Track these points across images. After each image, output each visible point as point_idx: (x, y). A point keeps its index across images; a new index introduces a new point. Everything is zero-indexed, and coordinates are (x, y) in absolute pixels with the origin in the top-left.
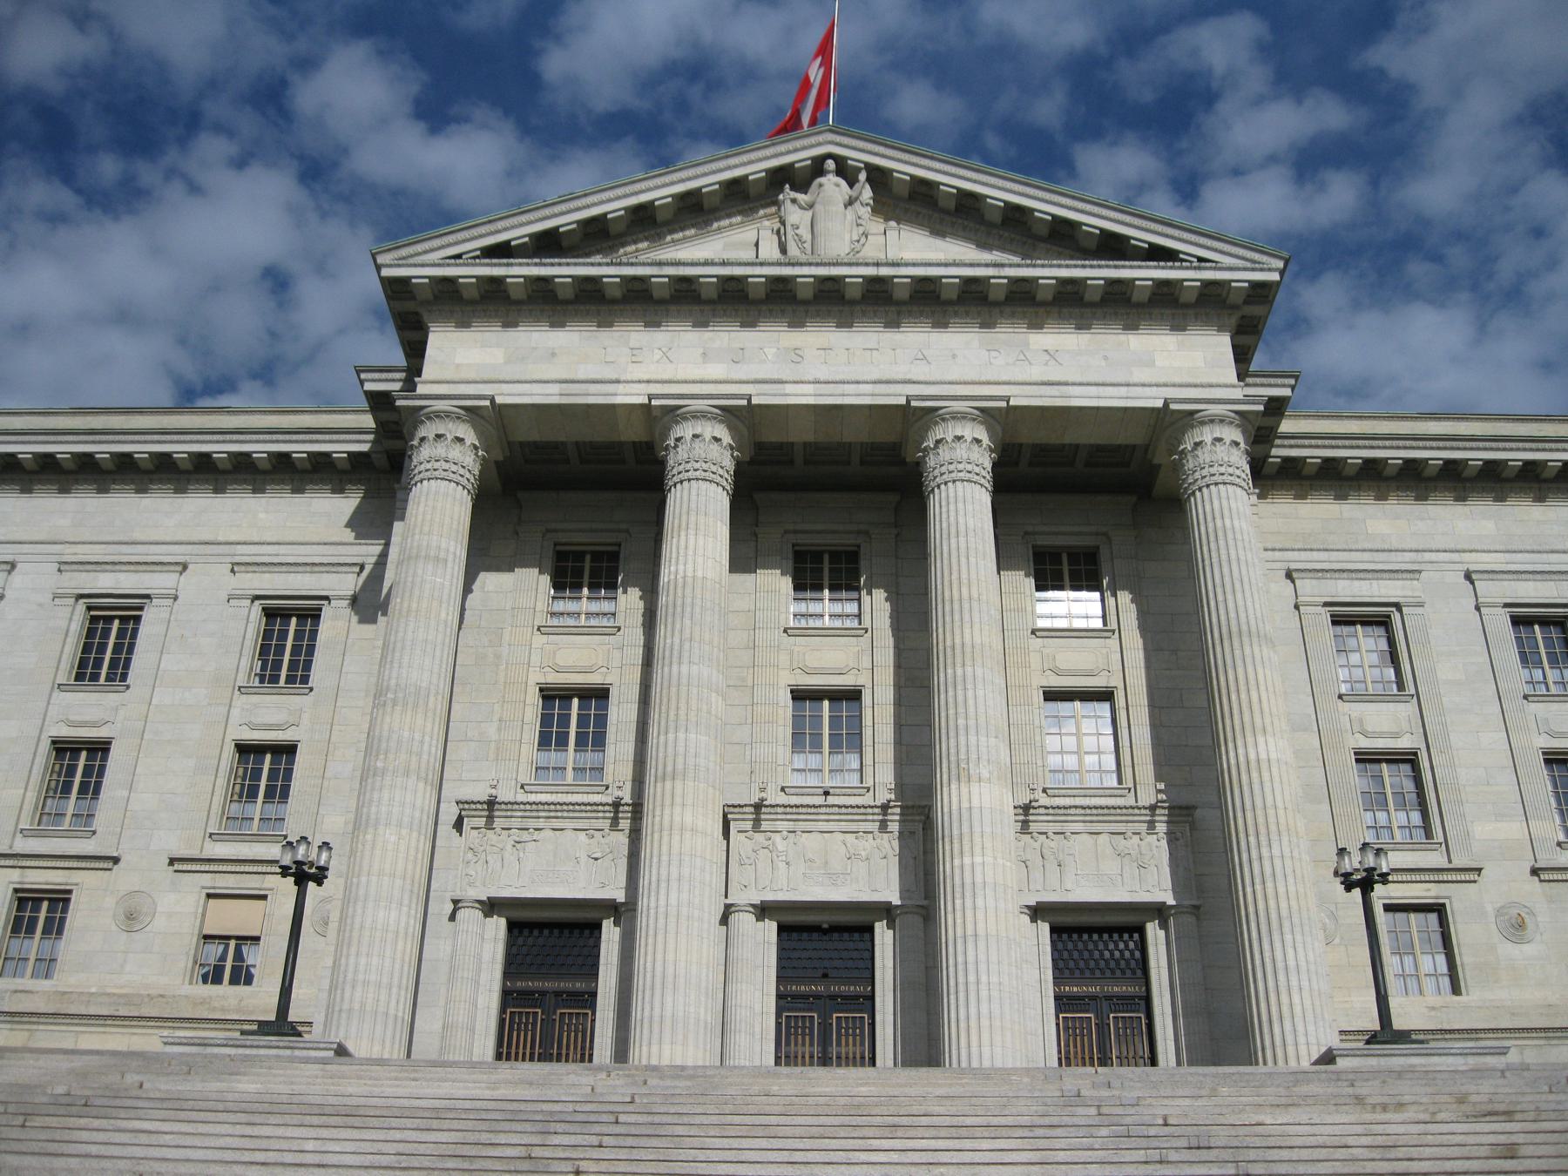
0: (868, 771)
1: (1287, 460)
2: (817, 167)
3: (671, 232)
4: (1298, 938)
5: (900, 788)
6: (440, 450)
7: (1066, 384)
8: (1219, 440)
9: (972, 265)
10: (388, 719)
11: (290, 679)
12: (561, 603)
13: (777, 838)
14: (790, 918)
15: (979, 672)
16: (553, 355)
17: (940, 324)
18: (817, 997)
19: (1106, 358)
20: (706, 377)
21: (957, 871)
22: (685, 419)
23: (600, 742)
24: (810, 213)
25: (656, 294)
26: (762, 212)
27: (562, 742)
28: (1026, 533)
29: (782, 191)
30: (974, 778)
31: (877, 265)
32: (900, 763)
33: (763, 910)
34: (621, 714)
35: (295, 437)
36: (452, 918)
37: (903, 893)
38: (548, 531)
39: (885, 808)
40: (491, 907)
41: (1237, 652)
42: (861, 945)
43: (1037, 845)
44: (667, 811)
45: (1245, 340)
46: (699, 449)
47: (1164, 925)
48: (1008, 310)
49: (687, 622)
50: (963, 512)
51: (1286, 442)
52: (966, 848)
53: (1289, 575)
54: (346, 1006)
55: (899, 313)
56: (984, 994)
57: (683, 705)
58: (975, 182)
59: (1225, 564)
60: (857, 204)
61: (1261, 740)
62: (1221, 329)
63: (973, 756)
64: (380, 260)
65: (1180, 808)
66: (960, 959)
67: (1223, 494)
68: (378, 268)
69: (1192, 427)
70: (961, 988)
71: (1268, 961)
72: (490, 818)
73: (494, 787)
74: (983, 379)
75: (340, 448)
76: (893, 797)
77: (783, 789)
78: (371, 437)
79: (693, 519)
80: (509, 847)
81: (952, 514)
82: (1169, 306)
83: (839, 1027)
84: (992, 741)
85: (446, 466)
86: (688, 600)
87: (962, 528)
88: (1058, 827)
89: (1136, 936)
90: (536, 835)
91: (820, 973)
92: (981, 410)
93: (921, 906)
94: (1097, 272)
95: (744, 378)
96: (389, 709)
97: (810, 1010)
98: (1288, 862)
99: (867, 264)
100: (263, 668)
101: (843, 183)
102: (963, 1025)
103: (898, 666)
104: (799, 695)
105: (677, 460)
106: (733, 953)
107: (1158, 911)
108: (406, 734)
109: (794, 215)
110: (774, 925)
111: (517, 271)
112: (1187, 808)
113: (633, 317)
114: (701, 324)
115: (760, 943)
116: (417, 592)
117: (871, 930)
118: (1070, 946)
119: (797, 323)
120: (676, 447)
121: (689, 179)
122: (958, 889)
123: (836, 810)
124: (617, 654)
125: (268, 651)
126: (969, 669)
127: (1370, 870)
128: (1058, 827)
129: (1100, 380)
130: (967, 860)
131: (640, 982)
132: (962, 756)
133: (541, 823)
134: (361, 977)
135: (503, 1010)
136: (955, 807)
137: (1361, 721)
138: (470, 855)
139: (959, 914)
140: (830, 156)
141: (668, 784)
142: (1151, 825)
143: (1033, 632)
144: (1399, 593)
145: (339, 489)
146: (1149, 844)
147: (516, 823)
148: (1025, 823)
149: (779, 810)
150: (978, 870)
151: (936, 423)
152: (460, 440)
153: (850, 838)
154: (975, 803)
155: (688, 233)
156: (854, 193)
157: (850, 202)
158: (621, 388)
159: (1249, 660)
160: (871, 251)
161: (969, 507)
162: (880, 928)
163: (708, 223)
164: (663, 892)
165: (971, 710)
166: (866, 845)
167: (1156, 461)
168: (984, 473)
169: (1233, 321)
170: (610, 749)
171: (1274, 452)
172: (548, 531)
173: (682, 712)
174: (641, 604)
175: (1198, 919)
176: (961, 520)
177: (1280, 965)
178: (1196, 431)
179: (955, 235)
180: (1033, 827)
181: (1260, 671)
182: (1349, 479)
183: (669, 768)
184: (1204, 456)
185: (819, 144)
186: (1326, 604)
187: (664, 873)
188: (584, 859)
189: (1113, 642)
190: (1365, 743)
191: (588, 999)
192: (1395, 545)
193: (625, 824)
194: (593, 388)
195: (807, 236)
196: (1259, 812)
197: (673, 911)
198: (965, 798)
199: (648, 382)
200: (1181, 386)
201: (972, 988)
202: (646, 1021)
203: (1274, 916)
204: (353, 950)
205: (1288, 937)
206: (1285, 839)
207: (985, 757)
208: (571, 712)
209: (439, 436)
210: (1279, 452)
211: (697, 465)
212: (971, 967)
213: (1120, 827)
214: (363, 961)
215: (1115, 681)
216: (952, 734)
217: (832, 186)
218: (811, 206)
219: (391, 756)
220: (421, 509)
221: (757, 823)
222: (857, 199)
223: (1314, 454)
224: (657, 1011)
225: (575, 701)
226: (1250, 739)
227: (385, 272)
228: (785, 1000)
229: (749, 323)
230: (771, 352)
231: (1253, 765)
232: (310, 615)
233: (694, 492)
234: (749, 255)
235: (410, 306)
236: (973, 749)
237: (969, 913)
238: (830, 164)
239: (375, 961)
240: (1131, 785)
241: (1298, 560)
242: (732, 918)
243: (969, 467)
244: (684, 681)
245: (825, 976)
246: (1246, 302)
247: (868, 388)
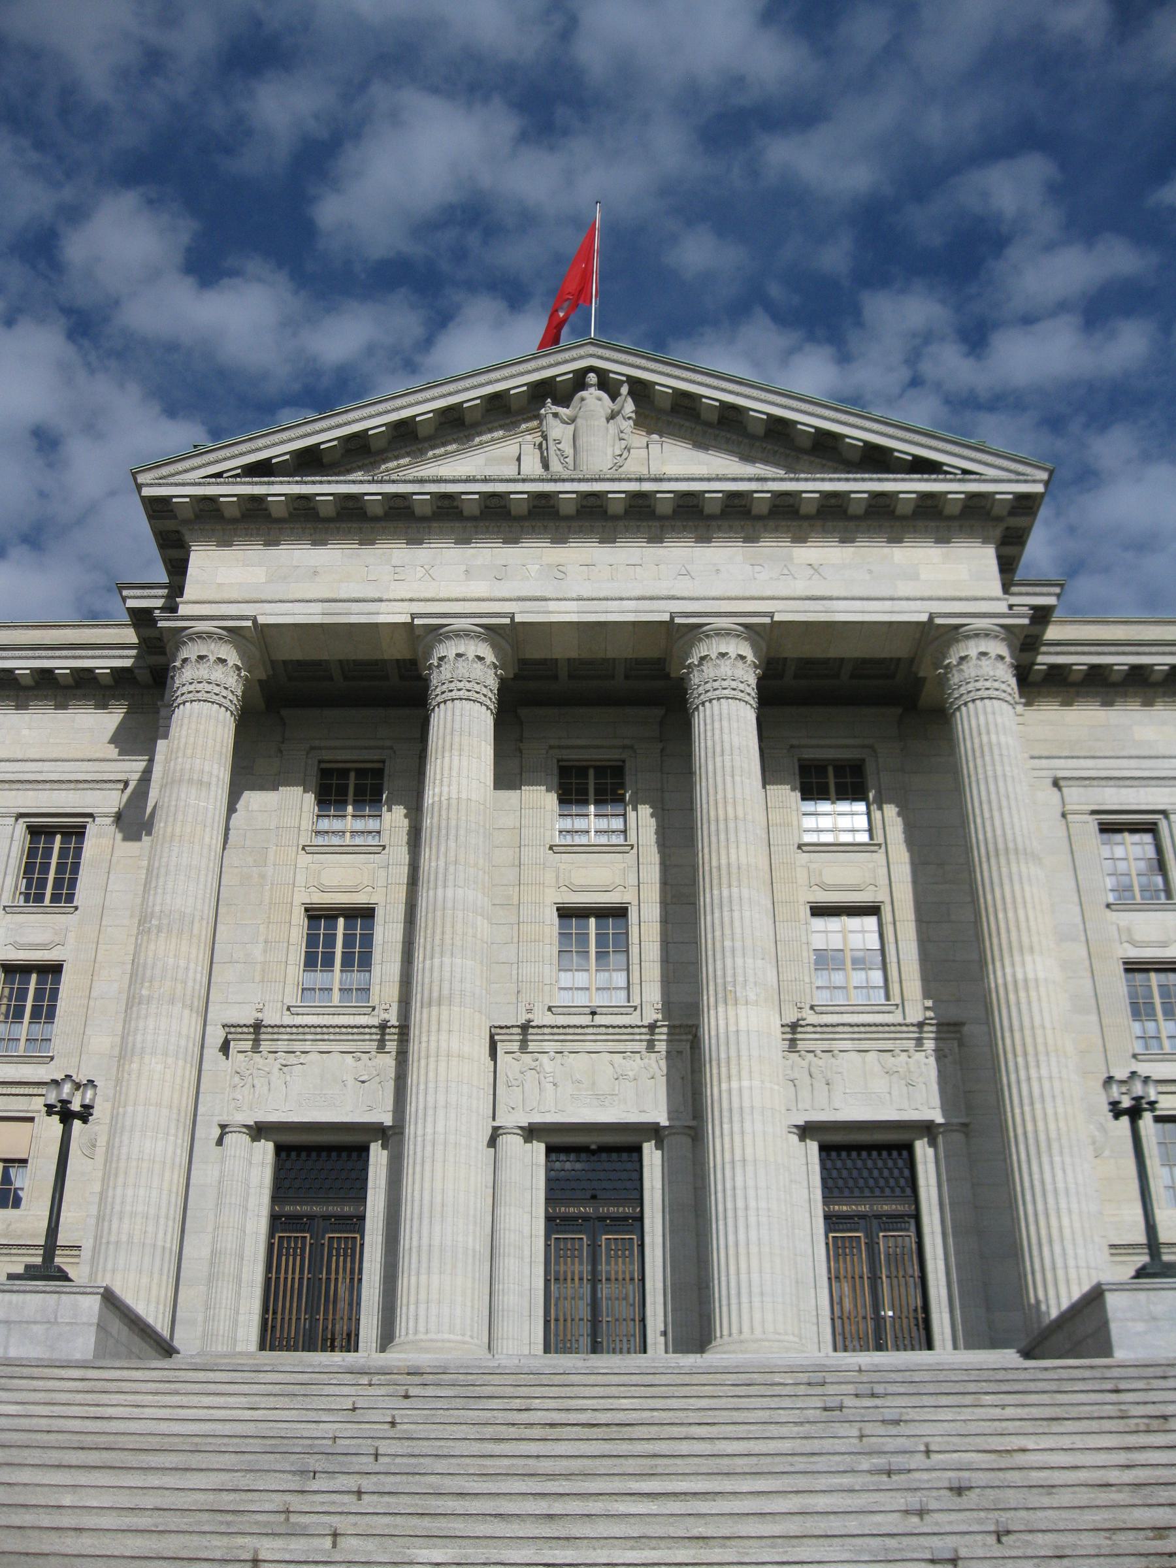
0: (635, 989)
1: (1053, 667)
2: (579, 381)
3: (433, 448)
4: (1068, 1160)
5: (668, 1006)
6: (203, 671)
7: (830, 599)
8: (984, 654)
9: (734, 480)
10: (152, 946)
11: (55, 898)
12: (326, 821)
13: (544, 1059)
14: (557, 1140)
15: (745, 892)
16: (315, 573)
17: (704, 538)
18: (586, 1218)
19: (870, 572)
20: (469, 595)
21: (725, 1095)
22: (448, 638)
23: (366, 962)
24: (572, 427)
25: (418, 511)
26: (524, 426)
27: (328, 962)
28: (792, 747)
29: (544, 406)
30: (741, 1001)
31: (640, 480)
32: (667, 981)
33: (531, 1132)
34: (387, 934)
35: (58, 653)
36: (220, 1142)
37: (672, 1113)
38: (312, 748)
39: (652, 1027)
40: (259, 1131)
41: (1004, 870)
42: (629, 1166)
43: (804, 1064)
44: (433, 1038)
45: (1009, 550)
46: (462, 668)
47: (933, 1143)
48: (771, 524)
49: (452, 844)
50: (728, 730)
51: (1052, 649)
52: (734, 1071)
53: (1056, 783)
54: (113, 1239)
55: (662, 527)
56: (752, 1220)
57: (448, 929)
58: (738, 394)
59: (991, 781)
60: (619, 418)
61: (1028, 958)
62: (986, 541)
63: (740, 979)
64: (141, 479)
65: (949, 1024)
66: (729, 1185)
67: (989, 710)
68: (139, 487)
69: (957, 641)
70: (730, 1214)
71: (1037, 1183)
72: (257, 1042)
73: (260, 1011)
74: (747, 594)
75: (102, 664)
76: (660, 1016)
77: (550, 1009)
78: (134, 652)
79: (456, 739)
80: (275, 1070)
81: (717, 732)
82: (932, 519)
83: (609, 1249)
84: (759, 962)
85: (209, 688)
86: (453, 823)
87: (727, 746)
88: (826, 1045)
89: (905, 1153)
90: (303, 1058)
91: (588, 1194)
92: (746, 626)
93: (689, 1125)
94: (860, 486)
95: (507, 595)
96: (153, 937)
97: (580, 1232)
98: (1056, 1083)
99: (630, 480)
100: (28, 887)
102: (732, 1251)
103: (664, 883)
104: (566, 913)
106: (503, 1176)
107: (927, 1129)
108: (171, 961)
109: (557, 430)
110: (542, 1147)
111: (280, 489)
112: (955, 1024)
113: (394, 535)
114: (464, 541)
115: (528, 1165)
116: (180, 817)
117: (639, 1150)
118: (839, 1164)
119: (559, 539)
120: (439, 666)
121: (450, 394)
122: (726, 1114)
123: (603, 1030)
124: (382, 873)
125: (33, 868)
126: (735, 890)
127: (1138, 1099)
128: (826, 1045)
130: (735, 1084)
131: (408, 1211)
132: (729, 979)
133: (307, 1046)
134: (128, 1208)
135: (271, 1235)
136: (722, 1030)
137: (1129, 930)
138: (237, 1079)
139: (727, 1139)
140: (591, 369)
141: (434, 1009)
142: (919, 1041)
143: (800, 847)
144: (1166, 800)
145: (102, 705)
146: (918, 1062)
147: (282, 1046)
148: (793, 1042)
149: (547, 1031)
150: (746, 1094)
151: (700, 640)
152: (222, 661)
153: (617, 1058)
154: (743, 1026)
155: (450, 448)
156: (616, 407)
157: (612, 416)
159: (1016, 878)
160: (634, 466)
161: (735, 725)
162: (649, 1148)
163: (470, 438)
164: (430, 1119)
165: (738, 931)
166: (634, 1065)
167: (921, 674)
168: (749, 690)
169: (998, 532)
170: (376, 969)
171: (1041, 659)
172: (312, 748)
173: (448, 937)
174: (406, 822)
175: (967, 1135)
176: (726, 737)
177: (1049, 1187)
178: (961, 645)
179: (718, 448)
180: (801, 1045)
181: (1027, 888)
182: (1114, 685)
183: (435, 995)
184: (969, 670)
185: (581, 357)
186: (1094, 812)
187: (431, 1099)
188: (351, 1082)
189: (880, 857)
190: (1134, 953)
191: (358, 1222)
192: (1162, 752)
193: (392, 1046)
194: (355, 607)
195: (569, 451)
196: (1027, 1033)
197: (440, 1138)
198: (732, 1021)
199: (411, 600)
200: (946, 599)
201: (740, 1213)
202: (414, 1250)
203: (1042, 1137)
204: (120, 1180)
205: (1057, 1159)
206: (1053, 1060)
207: (751, 979)
208: (336, 932)
209: (201, 658)
210: (1045, 659)
211: (460, 685)
212: (739, 1193)
213: (888, 1045)
214: (130, 1192)
215: (881, 896)
216: (719, 956)
217: (594, 399)
218: (573, 420)
219: (156, 984)
220: (184, 733)
221: (524, 1044)
222: (619, 412)
223: (1080, 660)
224: (425, 1241)
225: (341, 921)
226: (1017, 958)
227: (146, 492)
228: (553, 1222)
229: (512, 540)
230: (534, 569)
231: (1021, 985)
232: (73, 832)
233: (457, 712)
234: (510, 471)
235: (170, 525)
236: (739, 971)
237: (737, 1138)
238: (592, 378)
239: (142, 1192)
240: (898, 1001)
241: (1064, 768)
242: (501, 1140)
243: (734, 684)
244: (449, 905)
245: (594, 1197)
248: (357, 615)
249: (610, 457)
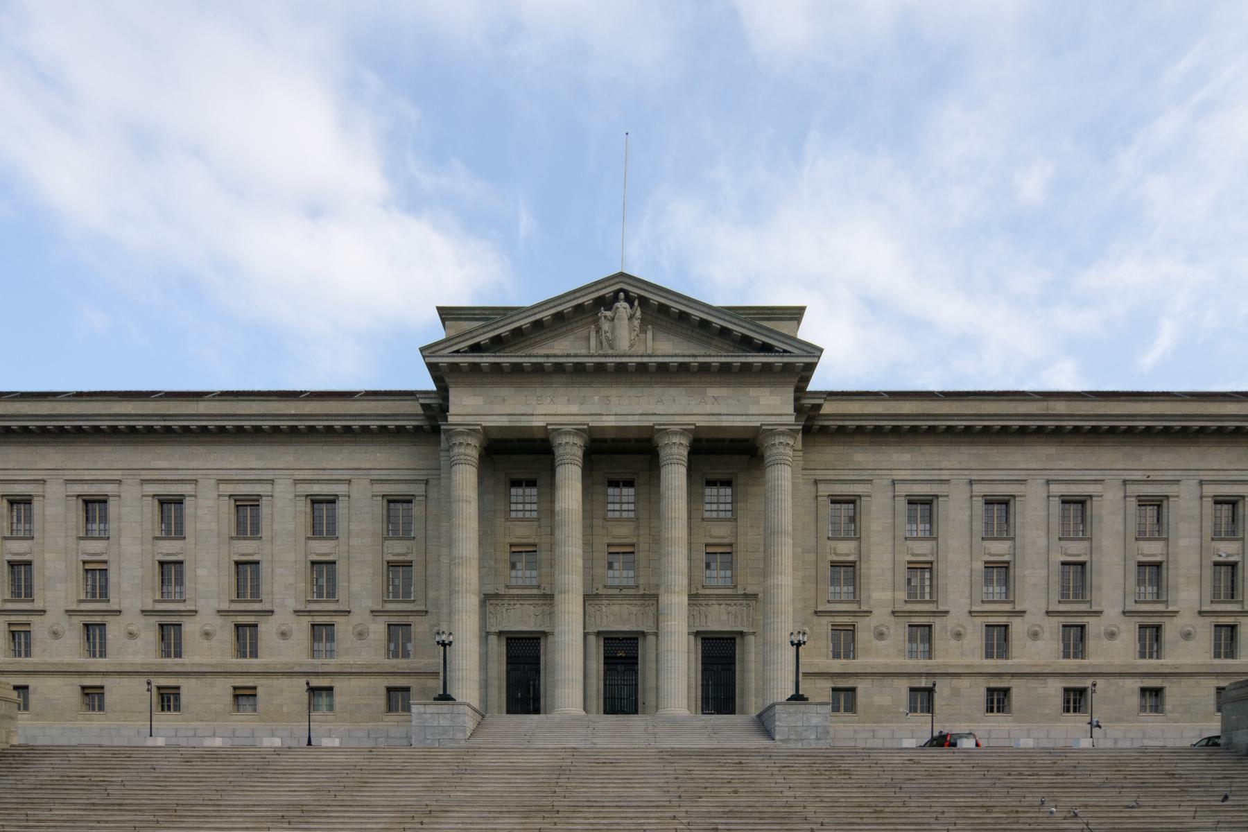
2: (615, 297)
6: (462, 450)
46: (568, 449)
101: (626, 305)
105: (559, 452)
109: (606, 326)
158: (534, 418)
160: (639, 349)
194: (522, 418)
217: (622, 305)
247: (637, 418)
248: (524, 422)
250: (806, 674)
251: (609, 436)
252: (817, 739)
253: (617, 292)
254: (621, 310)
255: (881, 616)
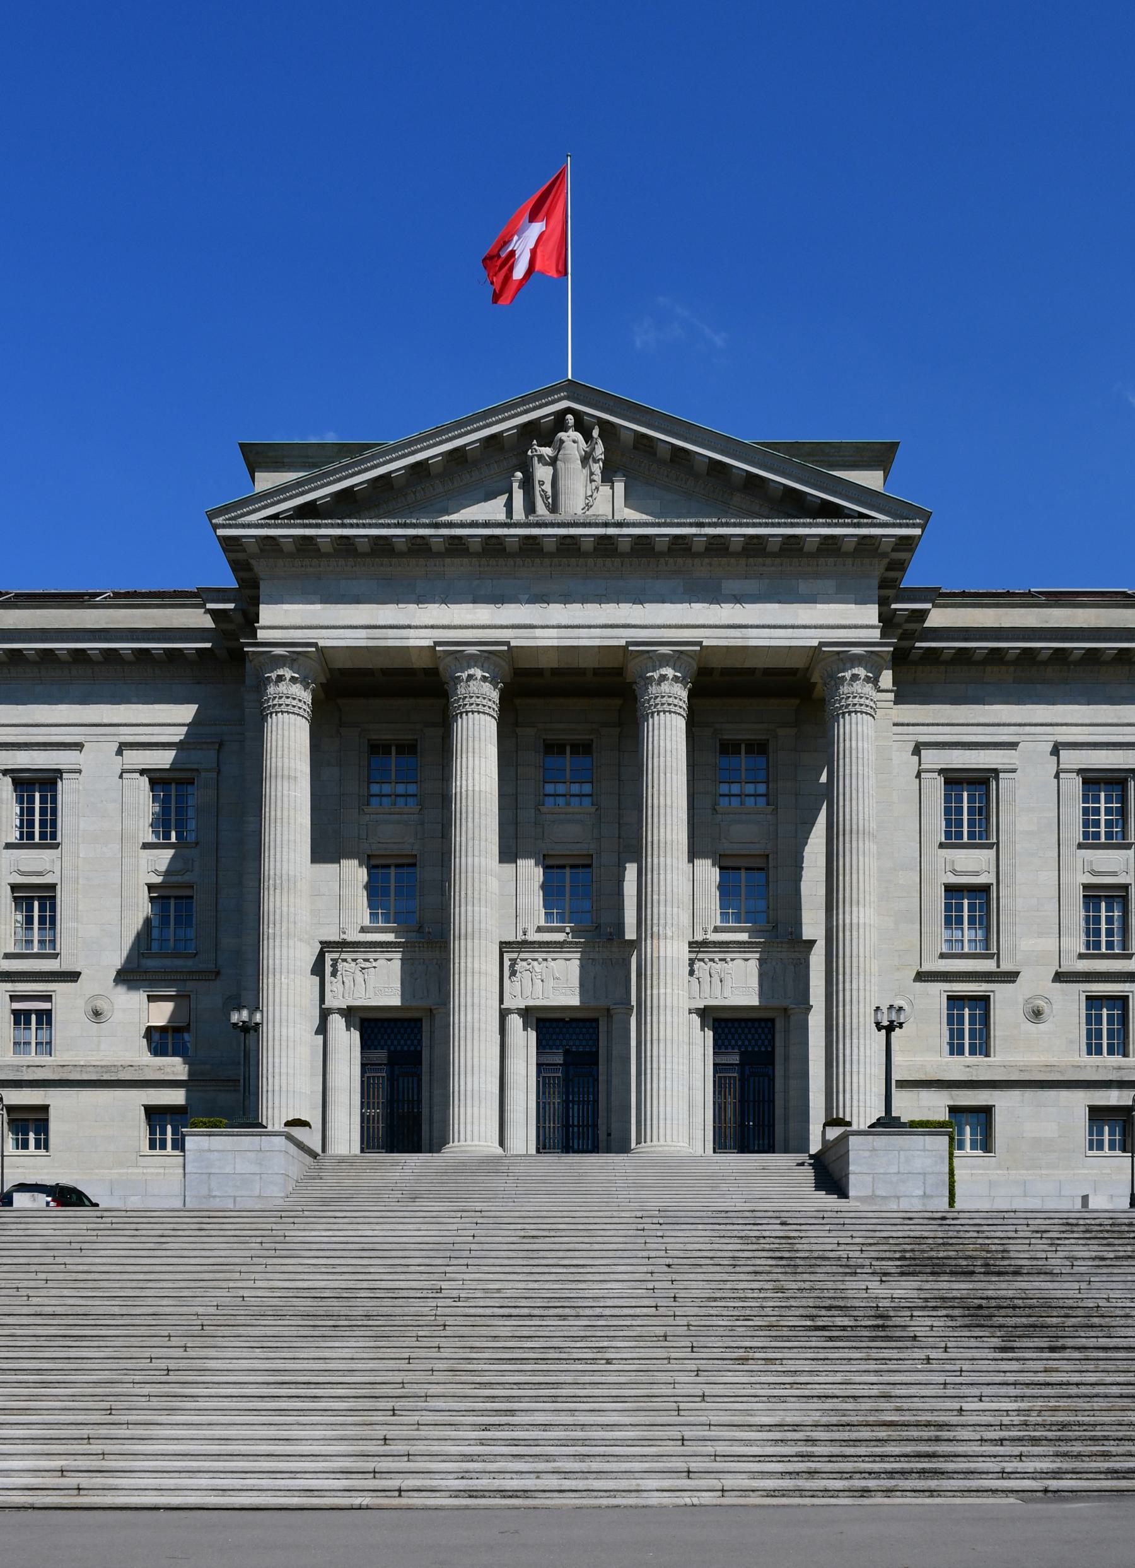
20: (476, 623)
25: (435, 548)
29: (530, 446)
43: (707, 967)
59: (847, 778)
89: (770, 1024)
95: (504, 623)
101: (579, 436)
129: (773, 623)
140: (569, 410)
246: (893, 550)
249: (583, 497)
250: (903, 1084)
251: (546, 663)
252: (925, 1196)
253: (561, 415)
254: (568, 444)
255: (1036, 982)
